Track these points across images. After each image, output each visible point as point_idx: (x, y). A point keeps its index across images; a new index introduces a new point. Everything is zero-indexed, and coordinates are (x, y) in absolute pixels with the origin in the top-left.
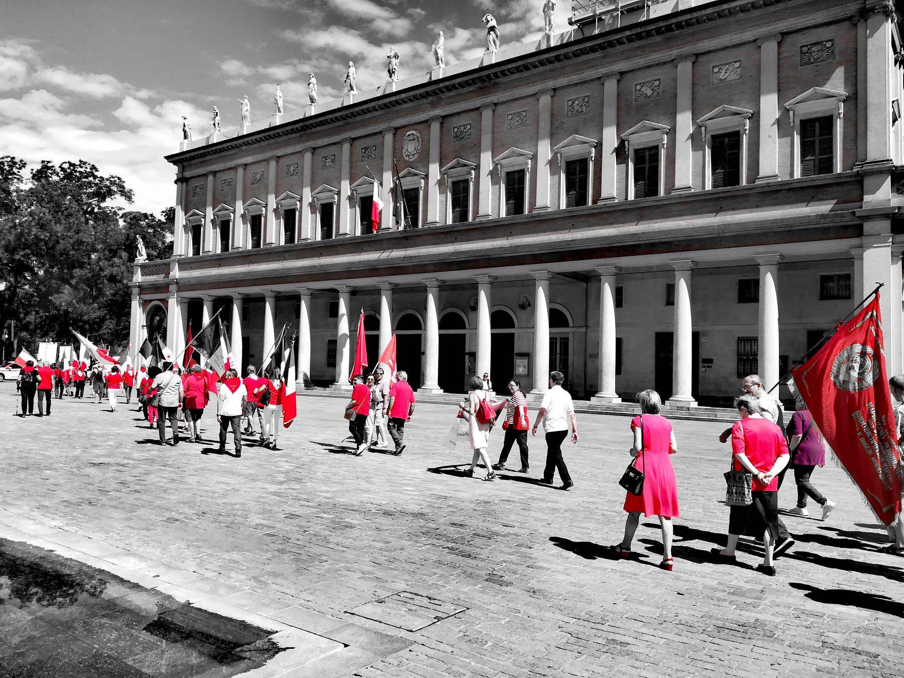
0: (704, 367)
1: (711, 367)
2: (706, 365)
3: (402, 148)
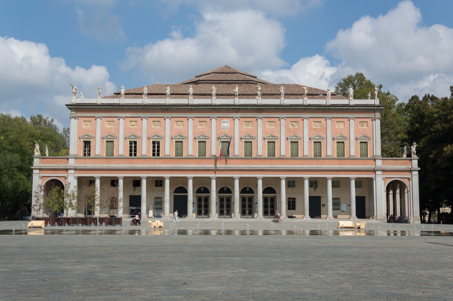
0: (322, 207)
1: (324, 207)
2: (323, 206)
3: (220, 125)
